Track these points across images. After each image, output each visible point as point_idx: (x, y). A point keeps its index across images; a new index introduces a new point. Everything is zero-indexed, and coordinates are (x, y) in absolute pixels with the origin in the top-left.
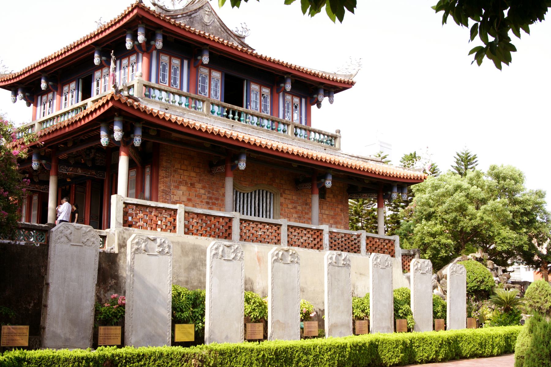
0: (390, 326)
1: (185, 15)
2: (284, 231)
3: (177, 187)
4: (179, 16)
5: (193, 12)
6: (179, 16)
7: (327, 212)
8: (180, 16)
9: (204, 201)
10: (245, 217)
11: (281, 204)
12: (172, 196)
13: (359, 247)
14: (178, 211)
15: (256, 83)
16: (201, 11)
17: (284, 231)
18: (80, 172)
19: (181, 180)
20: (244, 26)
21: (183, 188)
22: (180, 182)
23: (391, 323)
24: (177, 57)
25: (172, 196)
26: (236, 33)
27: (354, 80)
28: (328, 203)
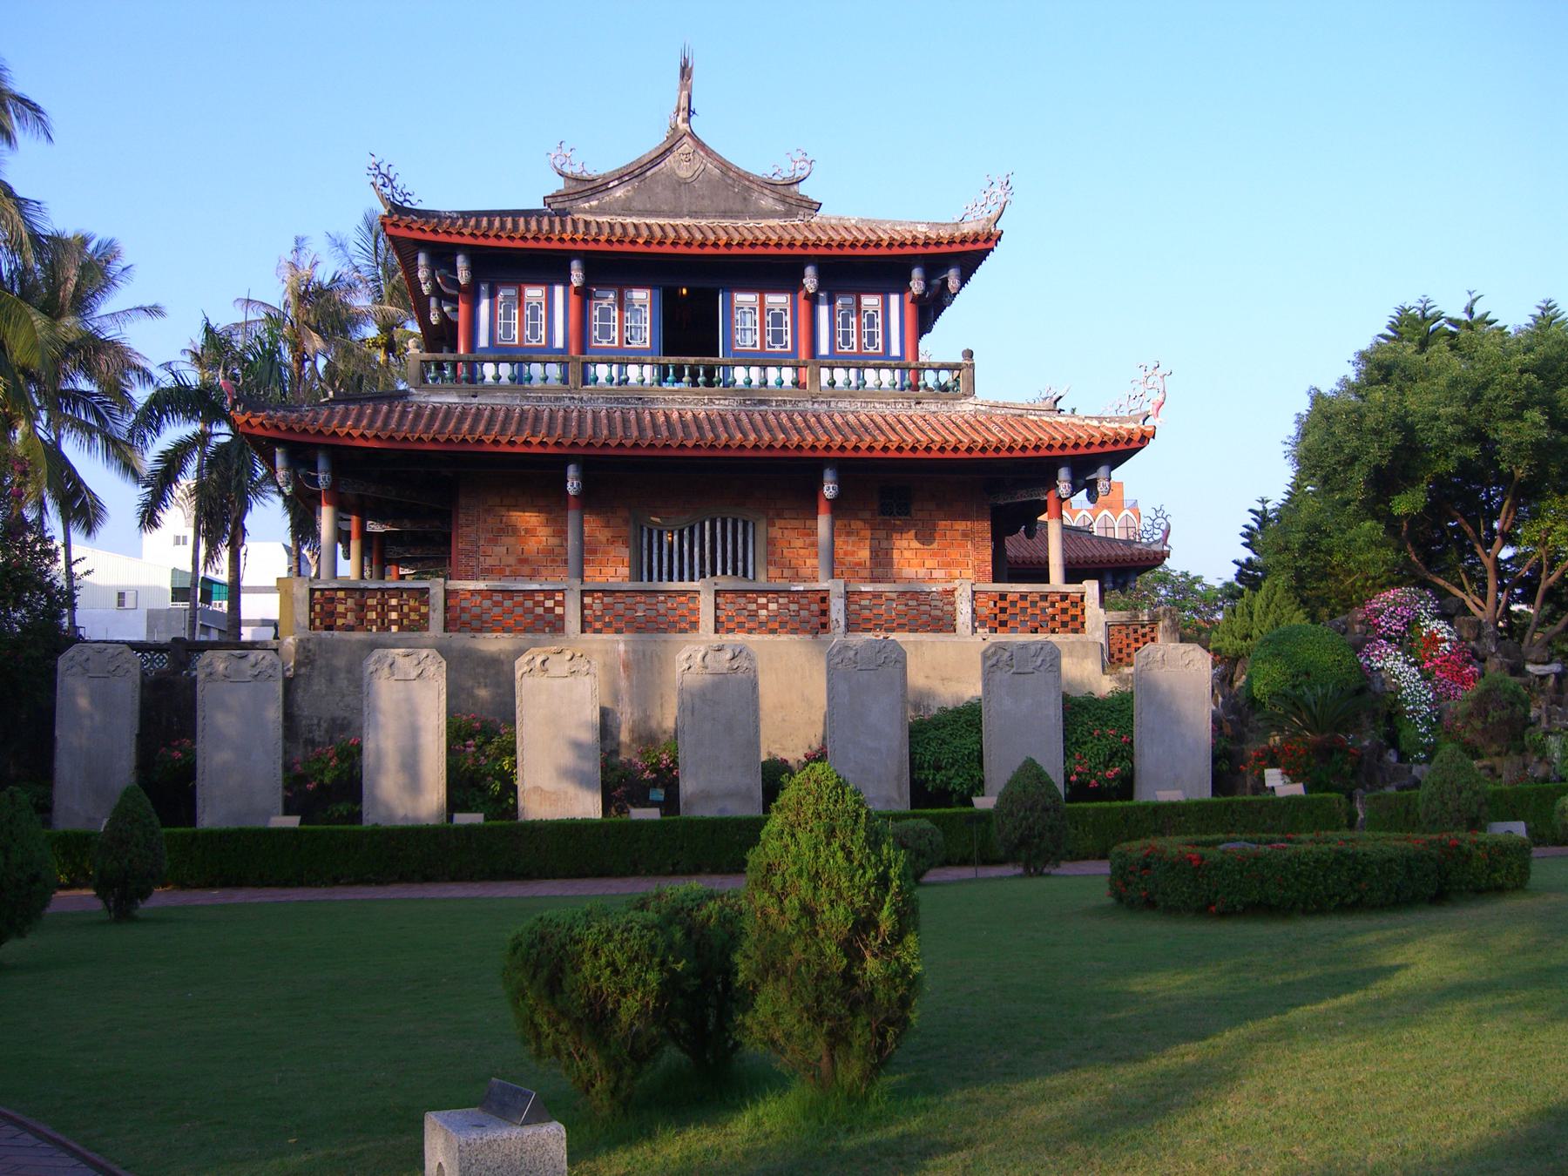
0: (896, 796)
1: (627, 178)
4: (611, 185)
5: (649, 166)
6: (611, 185)
8: (616, 183)
9: (559, 559)
12: (482, 559)
14: (431, 592)
16: (670, 161)
18: (408, 525)
19: (503, 526)
22: (501, 530)
23: (899, 788)
24: (535, 283)
25: (482, 559)
26: (776, 178)
28: (920, 523)
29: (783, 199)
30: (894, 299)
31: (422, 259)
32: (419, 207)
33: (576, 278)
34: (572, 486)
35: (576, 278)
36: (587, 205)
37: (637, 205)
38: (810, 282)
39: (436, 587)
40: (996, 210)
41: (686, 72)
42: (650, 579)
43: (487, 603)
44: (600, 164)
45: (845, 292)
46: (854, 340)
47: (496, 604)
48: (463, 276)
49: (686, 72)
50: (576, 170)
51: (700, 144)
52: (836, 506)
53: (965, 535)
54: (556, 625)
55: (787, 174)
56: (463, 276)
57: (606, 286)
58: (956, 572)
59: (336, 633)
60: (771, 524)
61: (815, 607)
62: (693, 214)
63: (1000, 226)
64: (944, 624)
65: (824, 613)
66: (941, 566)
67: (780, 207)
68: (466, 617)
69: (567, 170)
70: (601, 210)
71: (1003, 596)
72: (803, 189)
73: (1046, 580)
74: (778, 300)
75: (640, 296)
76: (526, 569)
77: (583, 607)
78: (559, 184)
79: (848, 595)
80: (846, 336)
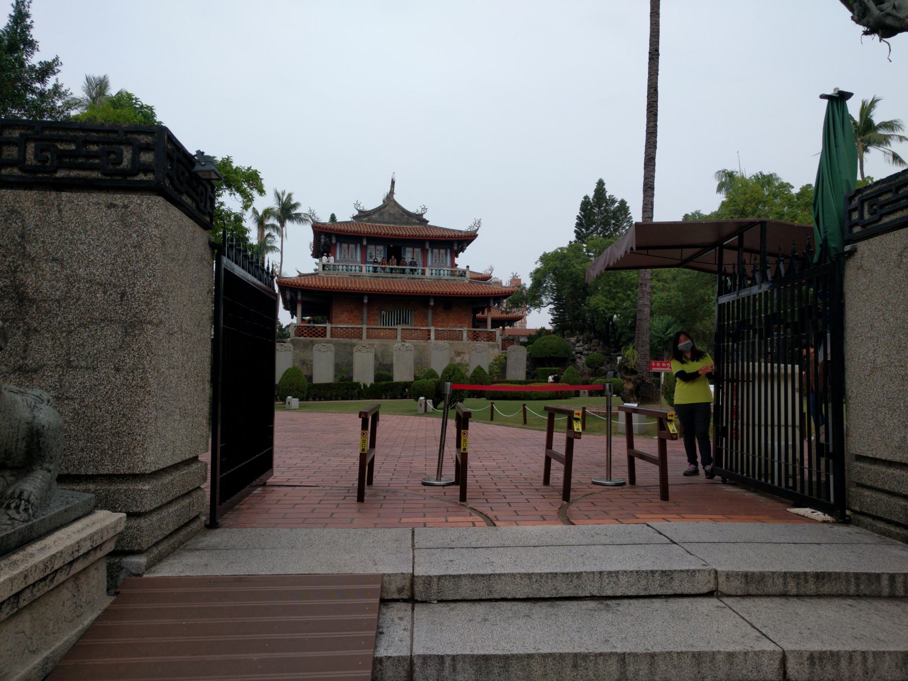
2: (399, 332)
7: (452, 317)
10: (369, 327)
11: (415, 316)
15: (409, 247)
17: (399, 332)
20: (423, 207)
21: (346, 314)
27: (477, 233)
29: (419, 220)
31: (323, 237)
32: (322, 222)
33: (365, 243)
34: (366, 301)
35: (365, 243)
36: (364, 219)
37: (378, 219)
38: (427, 246)
39: (328, 326)
40: (476, 228)
41: (393, 183)
42: (383, 325)
43: (342, 331)
45: (436, 248)
47: (344, 331)
48: (334, 241)
49: (393, 183)
50: (361, 209)
51: (396, 204)
52: (433, 308)
53: (466, 315)
54: (360, 338)
55: (420, 212)
56: (334, 241)
57: (371, 244)
58: (463, 325)
59: (301, 338)
60: (415, 311)
61: (427, 334)
62: (393, 223)
63: (477, 233)
64: (459, 338)
65: (429, 335)
66: (459, 323)
67: (417, 222)
68: (336, 334)
69: (359, 208)
70: (369, 221)
71: (475, 332)
72: (425, 217)
73: (486, 327)
74: (418, 250)
75: (380, 248)
76: (350, 321)
77: (367, 332)
78: (356, 213)
79: (436, 330)
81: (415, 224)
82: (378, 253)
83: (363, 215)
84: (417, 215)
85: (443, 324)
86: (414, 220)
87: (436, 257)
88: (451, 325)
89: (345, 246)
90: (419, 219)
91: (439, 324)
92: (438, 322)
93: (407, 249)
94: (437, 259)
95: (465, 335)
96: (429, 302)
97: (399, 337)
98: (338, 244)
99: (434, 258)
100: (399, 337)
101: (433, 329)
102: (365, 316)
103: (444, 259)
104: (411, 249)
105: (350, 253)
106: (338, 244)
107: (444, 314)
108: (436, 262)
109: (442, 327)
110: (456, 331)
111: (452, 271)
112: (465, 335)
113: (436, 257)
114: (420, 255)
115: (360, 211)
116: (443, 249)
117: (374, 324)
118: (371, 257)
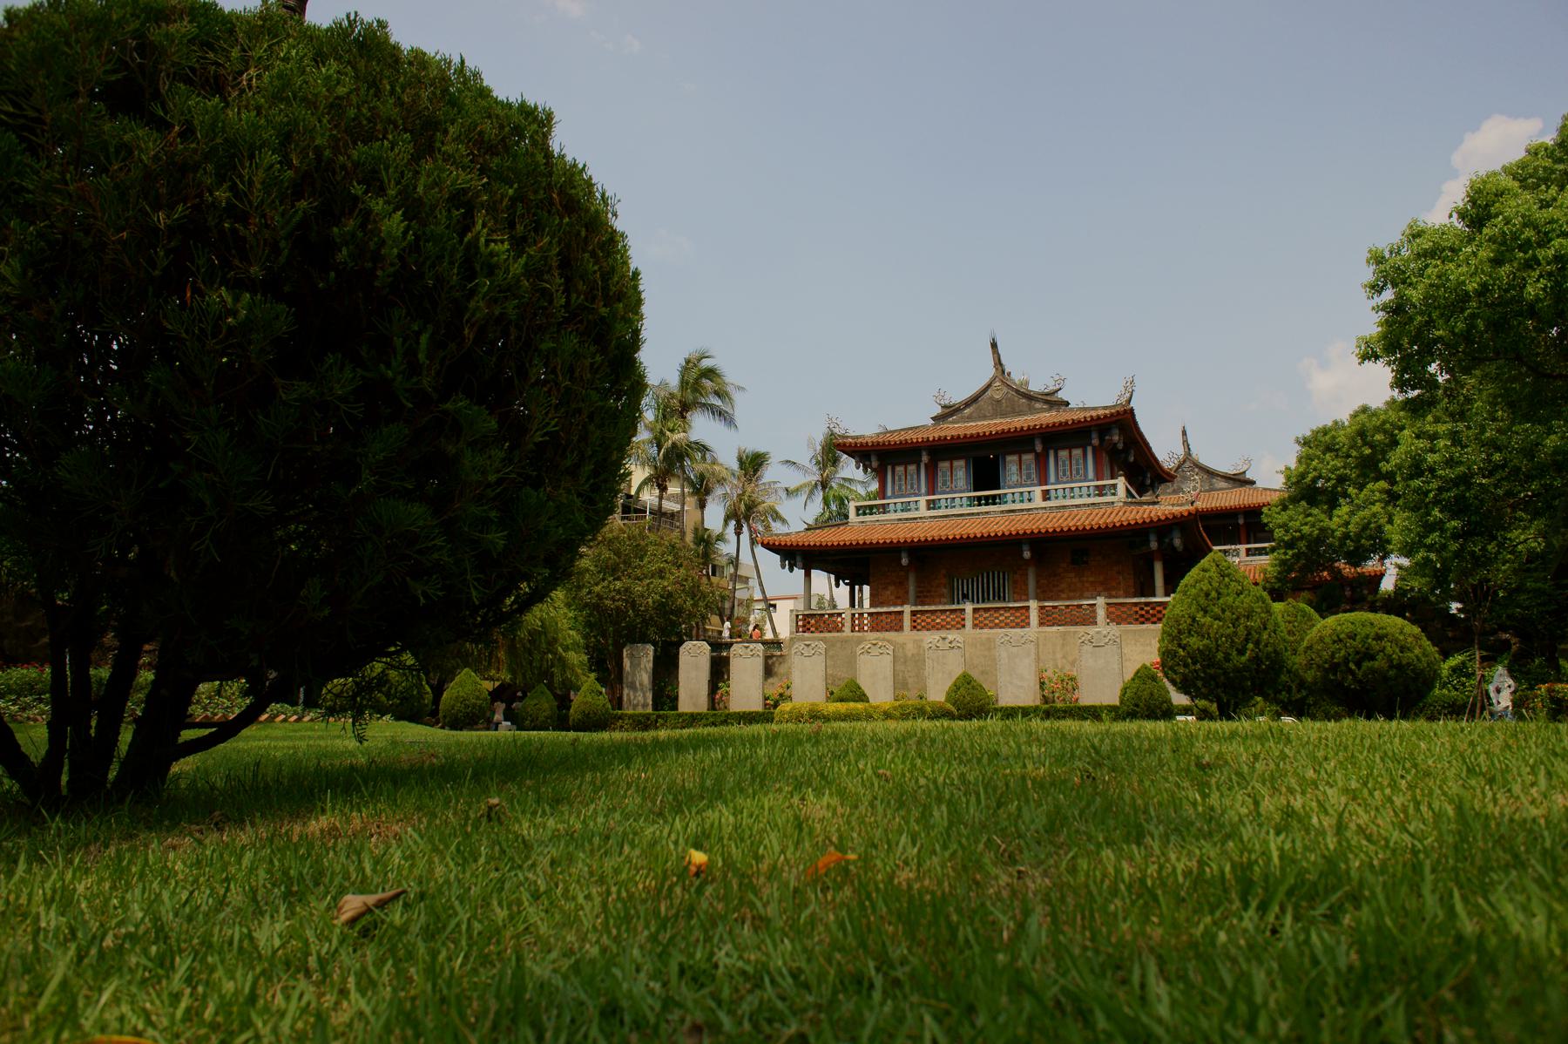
3: (885, 588)
7: (1091, 579)
11: (1015, 582)
13: (1095, 617)
20: (1057, 378)
21: (891, 588)
24: (912, 463)
30: (1089, 449)
40: (1128, 395)
41: (994, 345)
44: (958, 396)
46: (1081, 472)
53: (1119, 573)
55: (1052, 388)
63: (1132, 404)
64: (1090, 620)
72: (1061, 395)
75: (960, 463)
76: (899, 601)
78: (938, 410)
79: (1042, 608)
80: (1064, 471)
81: (1042, 410)
82: (961, 472)
83: (949, 412)
84: (1047, 394)
85: (1072, 594)
86: (1038, 405)
87: (1064, 465)
88: (1086, 594)
89: (900, 469)
90: (1051, 401)
91: (1063, 596)
92: (1062, 591)
93: (1009, 458)
94: (1068, 468)
95: (1101, 613)
96: (1022, 552)
97: (969, 623)
98: (889, 468)
99: (1061, 468)
100: (969, 623)
101: (1033, 605)
102: (912, 588)
103: (1081, 466)
104: (1015, 458)
105: (909, 482)
106: (889, 468)
107: (1072, 575)
108: (1078, 473)
109: (1069, 598)
110: (1080, 606)
111: (1097, 487)
112: (1101, 613)
113: (1064, 465)
114: (1033, 466)
115: (944, 407)
116: (1077, 447)
117: (940, 603)
118: (944, 483)
